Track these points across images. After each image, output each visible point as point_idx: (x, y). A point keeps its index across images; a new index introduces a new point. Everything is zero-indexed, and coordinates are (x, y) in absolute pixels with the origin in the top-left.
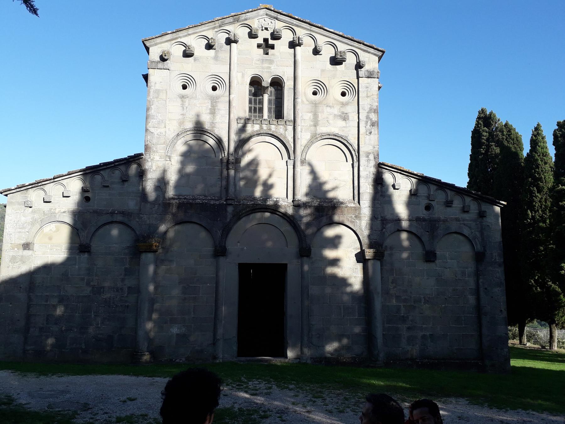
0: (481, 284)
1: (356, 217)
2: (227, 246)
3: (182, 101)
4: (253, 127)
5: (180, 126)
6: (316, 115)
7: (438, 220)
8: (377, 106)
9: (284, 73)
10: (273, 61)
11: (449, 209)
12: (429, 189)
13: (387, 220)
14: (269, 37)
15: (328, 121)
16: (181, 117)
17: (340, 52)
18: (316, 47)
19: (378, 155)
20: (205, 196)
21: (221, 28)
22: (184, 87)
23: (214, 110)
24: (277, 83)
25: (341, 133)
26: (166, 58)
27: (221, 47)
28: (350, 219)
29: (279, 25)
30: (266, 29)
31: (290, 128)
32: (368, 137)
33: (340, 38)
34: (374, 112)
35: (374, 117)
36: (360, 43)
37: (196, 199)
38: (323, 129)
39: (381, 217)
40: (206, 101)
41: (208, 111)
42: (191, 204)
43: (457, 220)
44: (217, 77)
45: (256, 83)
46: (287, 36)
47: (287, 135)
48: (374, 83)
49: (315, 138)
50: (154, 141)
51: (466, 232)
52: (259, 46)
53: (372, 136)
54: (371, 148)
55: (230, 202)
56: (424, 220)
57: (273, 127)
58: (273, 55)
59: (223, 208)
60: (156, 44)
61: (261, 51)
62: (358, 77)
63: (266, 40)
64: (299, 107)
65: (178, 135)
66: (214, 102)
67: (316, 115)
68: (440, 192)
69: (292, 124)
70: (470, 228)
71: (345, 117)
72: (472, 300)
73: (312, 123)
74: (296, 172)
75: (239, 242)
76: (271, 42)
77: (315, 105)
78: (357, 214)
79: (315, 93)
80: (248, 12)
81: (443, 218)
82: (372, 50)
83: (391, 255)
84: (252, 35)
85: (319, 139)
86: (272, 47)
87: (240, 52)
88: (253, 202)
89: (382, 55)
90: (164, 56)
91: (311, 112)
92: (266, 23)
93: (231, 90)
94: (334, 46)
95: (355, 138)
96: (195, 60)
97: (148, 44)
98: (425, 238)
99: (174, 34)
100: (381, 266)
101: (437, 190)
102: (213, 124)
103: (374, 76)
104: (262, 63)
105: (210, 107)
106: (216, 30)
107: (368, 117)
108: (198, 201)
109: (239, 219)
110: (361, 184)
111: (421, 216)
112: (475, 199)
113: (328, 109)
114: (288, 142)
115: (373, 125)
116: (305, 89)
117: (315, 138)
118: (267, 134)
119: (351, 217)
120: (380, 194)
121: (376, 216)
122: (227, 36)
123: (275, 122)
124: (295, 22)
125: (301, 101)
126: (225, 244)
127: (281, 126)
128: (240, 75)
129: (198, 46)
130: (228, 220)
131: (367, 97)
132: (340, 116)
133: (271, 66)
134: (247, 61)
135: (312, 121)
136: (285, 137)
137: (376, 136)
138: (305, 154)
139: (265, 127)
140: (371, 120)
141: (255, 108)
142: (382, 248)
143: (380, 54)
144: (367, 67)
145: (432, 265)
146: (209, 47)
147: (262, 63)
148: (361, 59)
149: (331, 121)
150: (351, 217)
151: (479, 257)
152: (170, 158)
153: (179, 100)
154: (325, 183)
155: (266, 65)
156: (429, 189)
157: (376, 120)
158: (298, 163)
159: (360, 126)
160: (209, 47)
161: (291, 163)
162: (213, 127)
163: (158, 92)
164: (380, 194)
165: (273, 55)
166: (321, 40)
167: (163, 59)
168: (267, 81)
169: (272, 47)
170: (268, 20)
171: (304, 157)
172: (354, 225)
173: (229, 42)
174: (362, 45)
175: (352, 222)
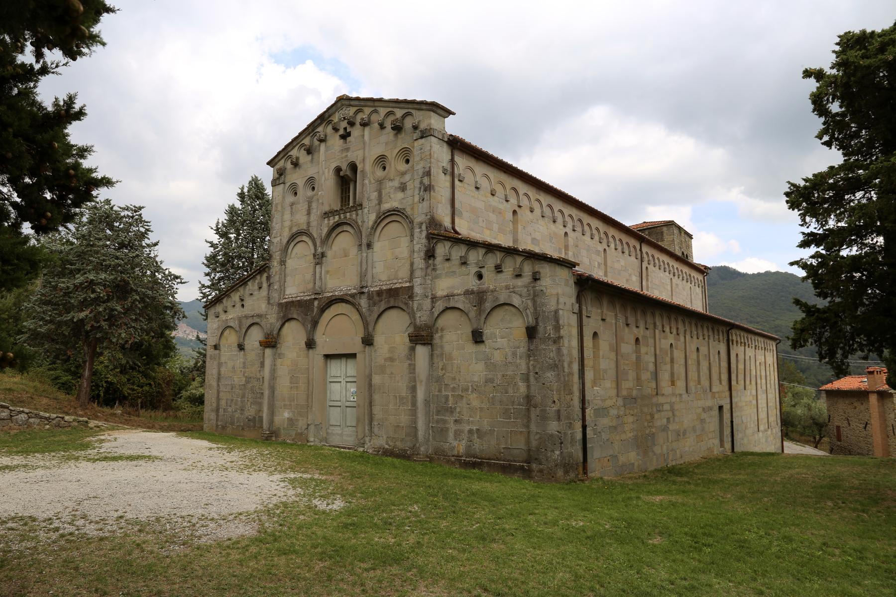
0: (531, 368)
11: (500, 276)
32: (421, 205)
33: (397, 105)
38: (386, 206)
42: (293, 302)
51: (516, 301)
56: (472, 292)
70: (521, 295)
71: (403, 188)
72: (522, 388)
77: (380, 182)
81: (492, 287)
83: (441, 337)
84: (336, 130)
101: (486, 253)
102: (308, 223)
120: (430, 269)
124: (362, 103)
128: (326, 171)
131: (422, 159)
132: (400, 187)
145: (481, 347)
149: (392, 196)
155: (344, 154)
164: (432, 267)
175: (406, 304)
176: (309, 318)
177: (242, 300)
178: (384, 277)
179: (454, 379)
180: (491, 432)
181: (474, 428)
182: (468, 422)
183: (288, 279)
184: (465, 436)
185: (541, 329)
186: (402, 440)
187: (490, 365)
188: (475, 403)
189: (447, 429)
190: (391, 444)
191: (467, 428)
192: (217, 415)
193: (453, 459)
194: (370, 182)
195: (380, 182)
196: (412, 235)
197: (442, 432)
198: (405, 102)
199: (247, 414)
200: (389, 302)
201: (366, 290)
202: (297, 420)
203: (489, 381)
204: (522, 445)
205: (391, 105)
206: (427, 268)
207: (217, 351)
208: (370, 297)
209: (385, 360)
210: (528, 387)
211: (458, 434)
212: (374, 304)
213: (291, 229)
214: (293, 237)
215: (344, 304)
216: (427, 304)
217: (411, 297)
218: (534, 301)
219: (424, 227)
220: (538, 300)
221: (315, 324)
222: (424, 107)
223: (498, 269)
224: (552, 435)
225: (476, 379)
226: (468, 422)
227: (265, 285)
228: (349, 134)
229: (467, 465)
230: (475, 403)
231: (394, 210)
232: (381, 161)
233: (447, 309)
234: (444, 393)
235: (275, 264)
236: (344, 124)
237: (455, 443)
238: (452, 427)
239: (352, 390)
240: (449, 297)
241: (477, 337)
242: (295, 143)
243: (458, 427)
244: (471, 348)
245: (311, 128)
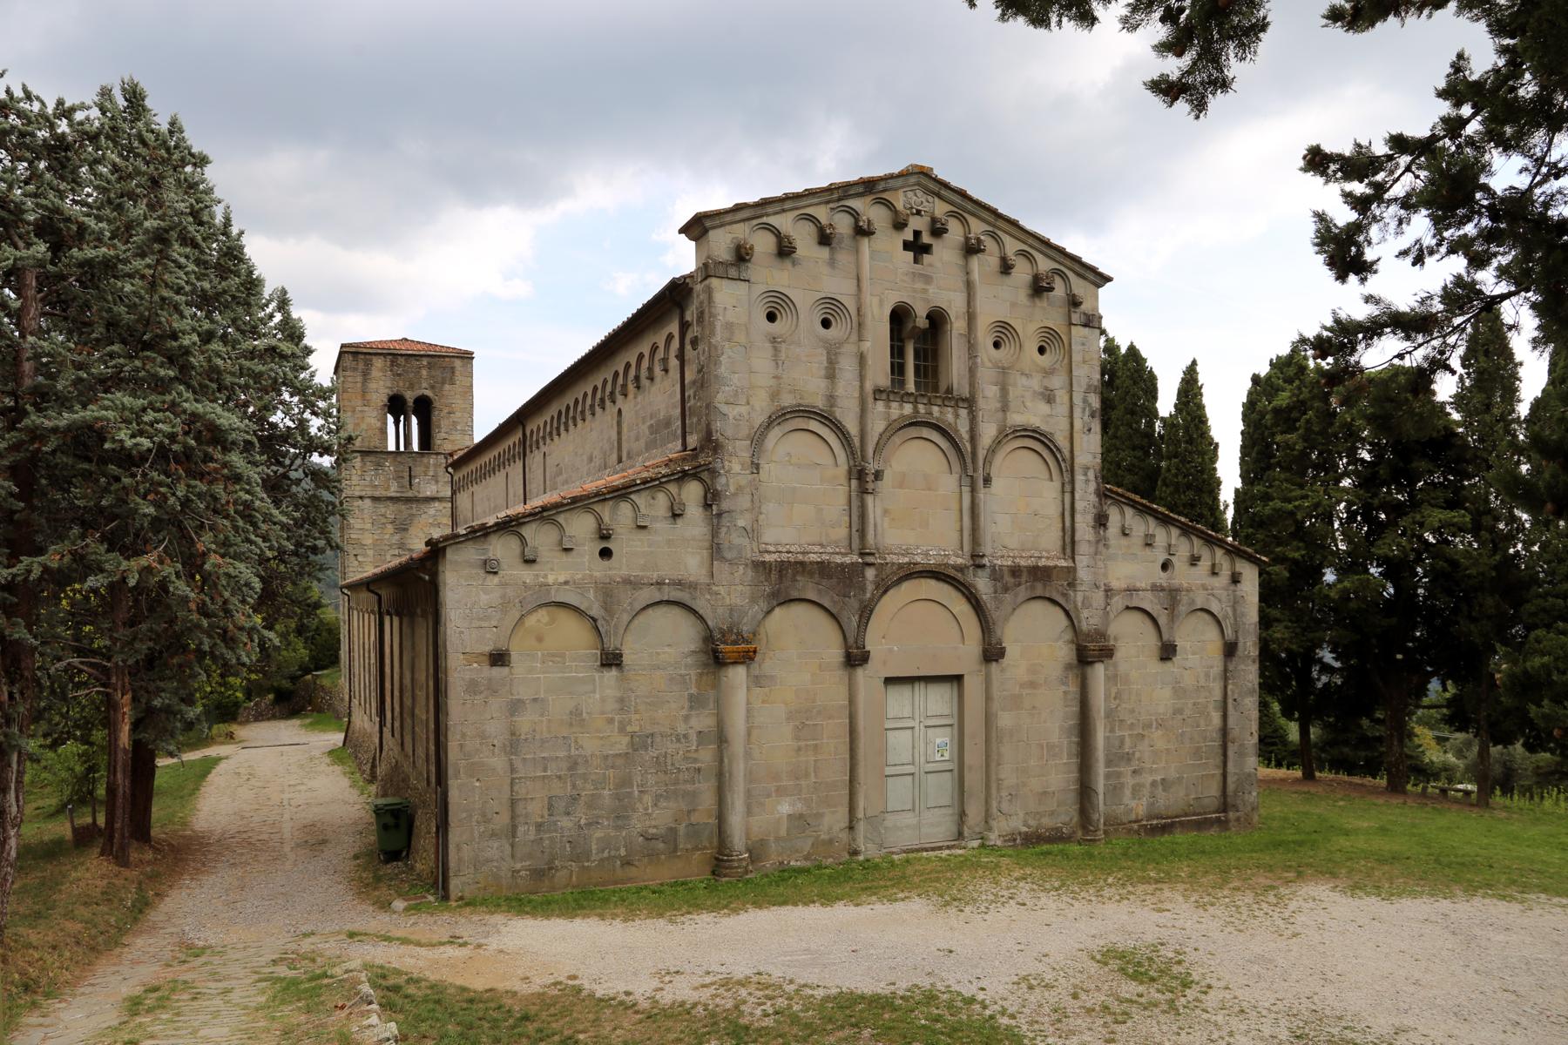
4: (901, 408)
6: (1004, 392)
7: (1178, 590)
12: (1169, 534)
16: (772, 382)
25: (1044, 428)
31: (963, 413)
32: (1085, 438)
38: (1016, 419)
41: (823, 372)
42: (802, 563)
43: (1204, 588)
50: (729, 433)
51: (1215, 608)
54: (1090, 457)
55: (870, 559)
56: (1163, 590)
57: (935, 409)
67: (1004, 392)
68: (1183, 539)
71: (1049, 399)
77: (1003, 371)
84: (899, 225)
88: (906, 560)
98: (1162, 621)
102: (831, 398)
107: (1085, 401)
108: (814, 557)
109: (885, 592)
110: (1077, 525)
111: (1158, 582)
112: (1228, 552)
114: (961, 438)
116: (985, 339)
132: (1042, 394)
136: (957, 431)
137: (1099, 437)
139: (922, 409)
148: (1075, 291)
149: (1028, 404)
151: (1230, 650)
155: (919, 285)
156: (1169, 534)
161: (966, 481)
175: (1065, 595)
176: (854, 603)
177: (605, 537)
178: (1013, 543)
179: (1132, 711)
180: (1180, 779)
181: (1158, 778)
182: (1151, 771)
183: (769, 508)
184: (1146, 791)
185: (1240, 645)
186: (1052, 813)
187: (1179, 691)
188: (1161, 744)
189: (1122, 785)
190: (1032, 822)
191: (1150, 779)
192: (512, 846)
193: (1135, 826)
196: (1072, 482)
197: (1115, 790)
198: (1061, 251)
199: (637, 824)
200: (1033, 588)
201: (985, 561)
202: (819, 816)
203: (1178, 711)
204: (1213, 790)
205: (1030, 241)
206: (1098, 542)
207: (505, 670)
208: (996, 574)
209: (1022, 686)
210: (1225, 717)
211: (1136, 790)
212: (1006, 589)
213: (774, 395)
214: (781, 416)
215: (933, 582)
216: (1098, 598)
217: (1072, 585)
218: (1234, 610)
219: (1091, 475)
220: (1239, 609)
221: (866, 613)
222: (1091, 276)
223: (1194, 560)
224: (1249, 775)
225: (1161, 710)
226: (1151, 771)
227: (694, 511)
228: (927, 249)
229: (1155, 830)
230: (1161, 744)
232: (1003, 334)
233: (1128, 608)
234: (1119, 733)
235: (736, 468)
237: (1133, 804)
238: (1129, 781)
239: (938, 741)
240: (1131, 590)
241: (1167, 652)
242: (788, 205)
243: (1138, 779)
244: (1155, 667)
245: (838, 193)
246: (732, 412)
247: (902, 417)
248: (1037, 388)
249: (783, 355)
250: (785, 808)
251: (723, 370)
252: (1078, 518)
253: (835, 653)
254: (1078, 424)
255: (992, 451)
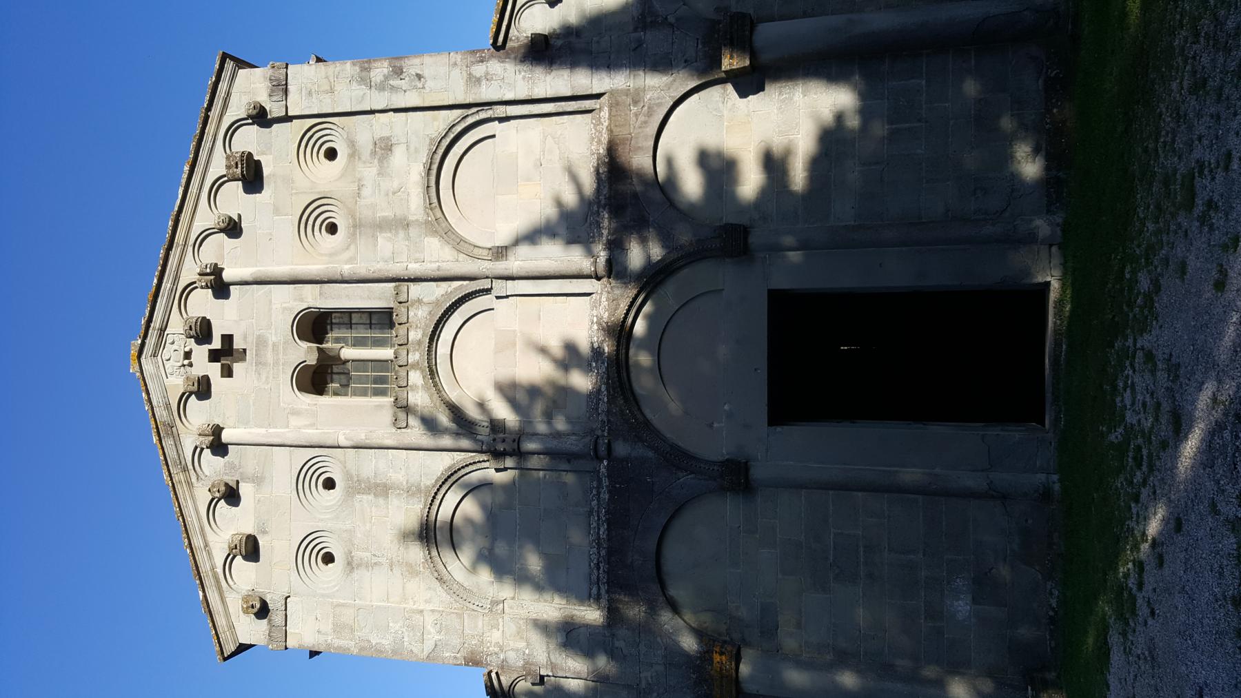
1: (635, 102)
2: (721, 459)
3: (359, 565)
4: (414, 388)
5: (418, 573)
6: (383, 225)
8: (354, 64)
9: (285, 309)
10: (259, 337)
13: (642, 14)
14: (207, 347)
15: (394, 193)
16: (397, 571)
17: (228, 167)
18: (221, 231)
19: (473, 52)
20: (590, 513)
21: (190, 467)
22: (329, 558)
23: (377, 485)
24: (314, 325)
25: (424, 157)
26: (258, 606)
27: (232, 466)
28: (641, 118)
29: (177, 326)
30: (188, 355)
31: (416, 290)
32: (430, 84)
34: (368, 70)
35: (380, 70)
36: (206, 119)
37: (599, 538)
38: (415, 203)
39: (635, 30)
40: (357, 505)
41: (381, 501)
42: (610, 553)
44: (302, 478)
45: (316, 379)
46: (202, 303)
47: (433, 299)
48: (303, 75)
49: (438, 225)
50: (456, 641)
52: (227, 372)
53: (426, 73)
54: (456, 72)
55: (602, 449)
57: (415, 335)
58: (245, 338)
59: (619, 469)
60: (232, 627)
61: (237, 367)
62: (287, 119)
63: (214, 356)
64: (362, 270)
65: (440, 579)
66: (360, 487)
67: (383, 225)
69: (404, 286)
71: (384, 148)
73: (401, 234)
74: (523, 274)
75: (711, 426)
76: (216, 344)
77: (357, 226)
78: (629, 100)
79: (332, 229)
80: (149, 400)
82: (223, 86)
84: (203, 389)
85: (439, 214)
86: (228, 339)
87: (243, 422)
89: (233, 58)
90: (255, 610)
91: (375, 238)
92: (174, 355)
93: (329, 443)
94: (218, 185)
95: (435, 119)
96: (264, 532)
97: (230, 648)
99: (207, 583)
100: (773, 20)
102: (411, 491)
103: (283, 77)
104: (265, 364)
105: (371, 497)
106: (194, 479)
107: (381, 87)
109: (647, 423)
113: (366, 192)
115: (398, 72)
116: (324, 255)
117: (438, 225)
118: (429, 351)
119: (636, 115)
120: (573, 39)
121: (633, 46)
122: (207, 452)
123: (402, 330)
124: (167, 285)
125: (350, 265)
126: (714, 463)
127: (411, 314)
128: (294, 421)
129: (233, 523)
130: (651, 454)
131: (332, 91)
132: (380, 161)
133: (270, 343)
134: (260, 403)
135: (397, 233)
136: (437, 303)
137: (428, 59)
138: (476, 250)
140: (386, 78)
141: (378, 380)
142: (719, 22)
143: (229, 65)
144: (263, 98)
146: (232, 496)
147: (265, 364)
149: (396, 185)
150: (636, 115)
152: (497, 603)
153: (356, 575)
154: (559, 203)
155: (269, 356)
157: (386, 64)
158: (501, 267)
159: (403, 106)
160: (232, 496)
161: (500, 287)
162: (419, 490)
163: (338, 628)
164: (573, 39)
165: (245, 338)
166: (205, 218)
167: (263, 611)
168: (305, 352)
169: (228, 339)
170: (168, 352)
171: (485, 252)
172: (659, 105)
173: (219, 448)
174: (211, 114)
175: (650, 114)
194: (351, 260)
195: (357, 226)
231: (428, 174)
236: (201, 353)
246: (433, 636)
247: (426, 388)
248: (374, 170)
249: (365, 555)
250: (962, 607)
251: (386, 642)
252: (539, 93)
253: (728, 509)
254: (412, 100)
255: (459, 243)
